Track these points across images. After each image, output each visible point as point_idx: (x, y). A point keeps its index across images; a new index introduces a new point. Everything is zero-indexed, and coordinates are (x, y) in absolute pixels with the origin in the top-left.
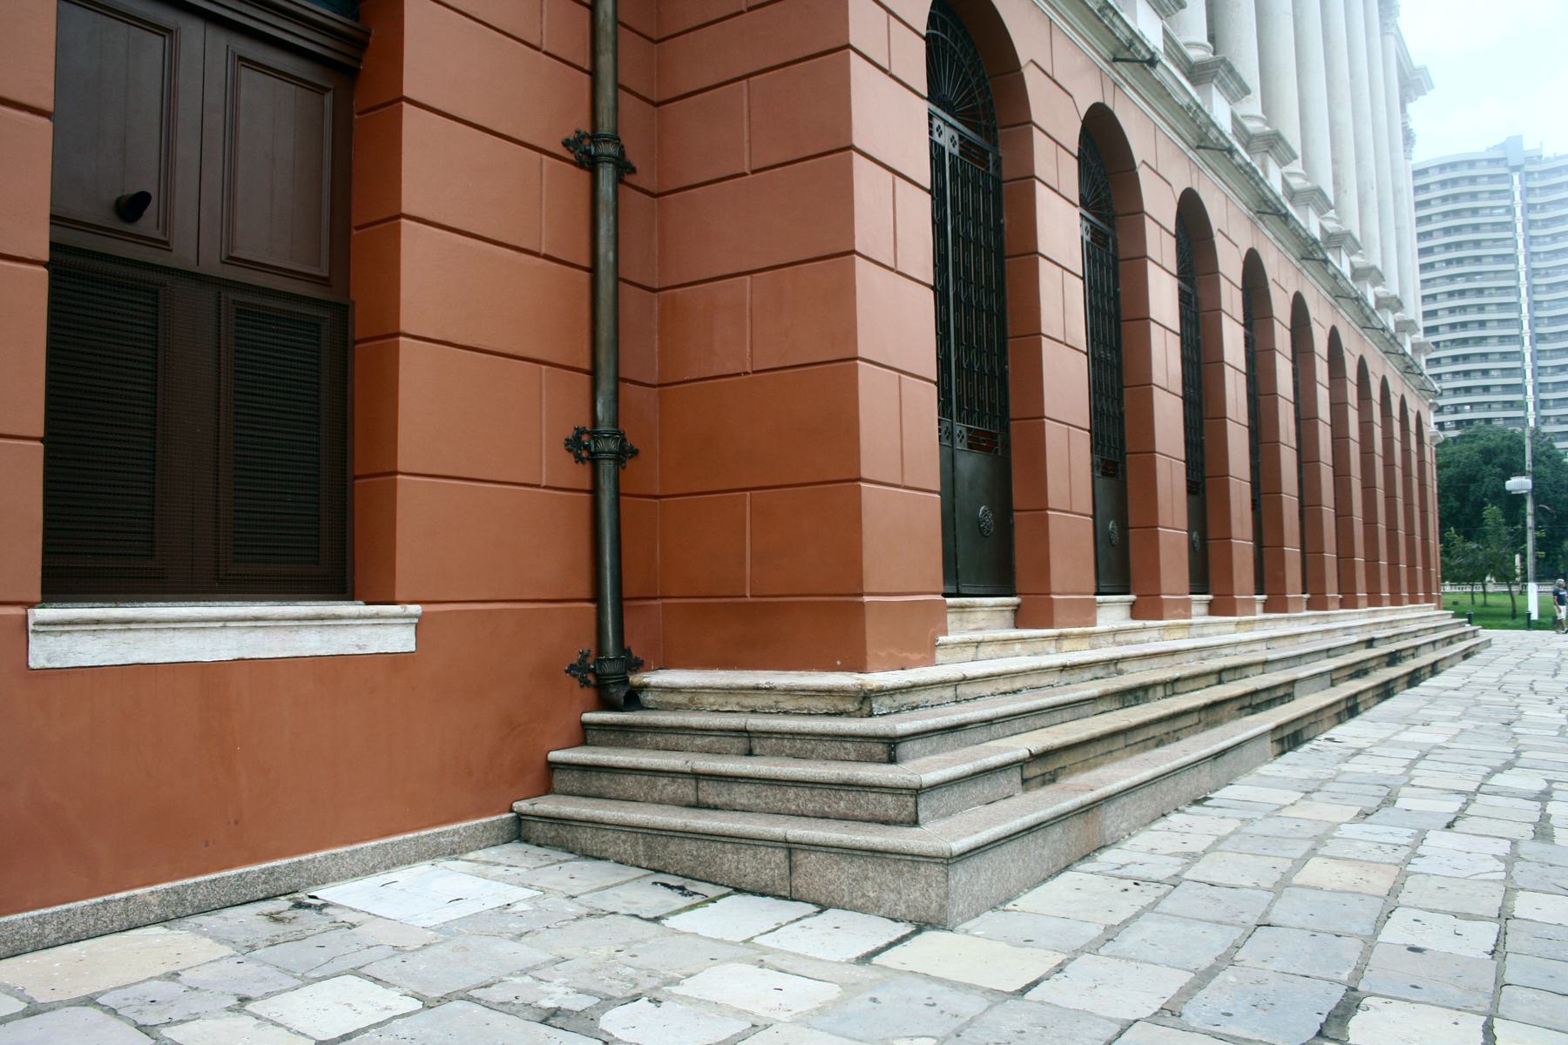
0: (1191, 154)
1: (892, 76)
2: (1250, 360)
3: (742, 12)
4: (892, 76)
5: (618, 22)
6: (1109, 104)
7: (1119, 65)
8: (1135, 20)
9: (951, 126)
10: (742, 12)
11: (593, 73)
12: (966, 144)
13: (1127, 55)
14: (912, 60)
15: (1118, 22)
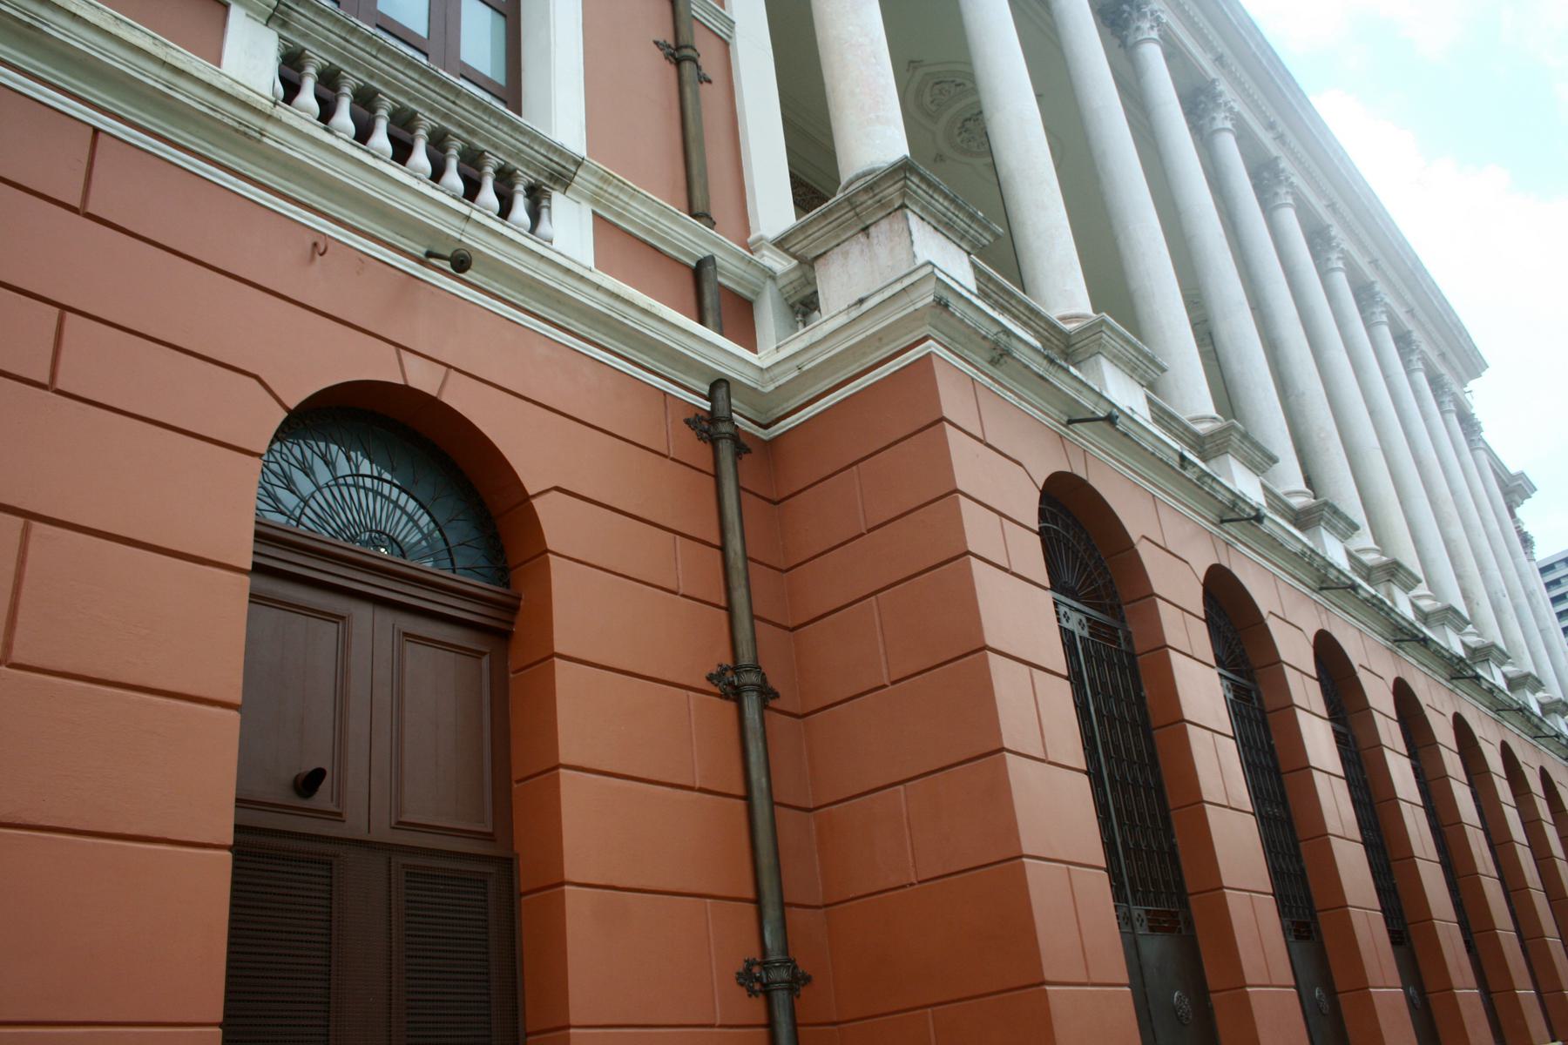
0: (1315, 596)
1: (1013, 574)
2: (1458, 906)
4: (1013, 574)
5: (747, 558)
6: (1226, 564)
7: (1227, 526)
8: (1233, 481)
9: (1077, 610)
11: (729, 609)
12: (1094, 625)
14: (1030, 555)
15: (1217, 487)
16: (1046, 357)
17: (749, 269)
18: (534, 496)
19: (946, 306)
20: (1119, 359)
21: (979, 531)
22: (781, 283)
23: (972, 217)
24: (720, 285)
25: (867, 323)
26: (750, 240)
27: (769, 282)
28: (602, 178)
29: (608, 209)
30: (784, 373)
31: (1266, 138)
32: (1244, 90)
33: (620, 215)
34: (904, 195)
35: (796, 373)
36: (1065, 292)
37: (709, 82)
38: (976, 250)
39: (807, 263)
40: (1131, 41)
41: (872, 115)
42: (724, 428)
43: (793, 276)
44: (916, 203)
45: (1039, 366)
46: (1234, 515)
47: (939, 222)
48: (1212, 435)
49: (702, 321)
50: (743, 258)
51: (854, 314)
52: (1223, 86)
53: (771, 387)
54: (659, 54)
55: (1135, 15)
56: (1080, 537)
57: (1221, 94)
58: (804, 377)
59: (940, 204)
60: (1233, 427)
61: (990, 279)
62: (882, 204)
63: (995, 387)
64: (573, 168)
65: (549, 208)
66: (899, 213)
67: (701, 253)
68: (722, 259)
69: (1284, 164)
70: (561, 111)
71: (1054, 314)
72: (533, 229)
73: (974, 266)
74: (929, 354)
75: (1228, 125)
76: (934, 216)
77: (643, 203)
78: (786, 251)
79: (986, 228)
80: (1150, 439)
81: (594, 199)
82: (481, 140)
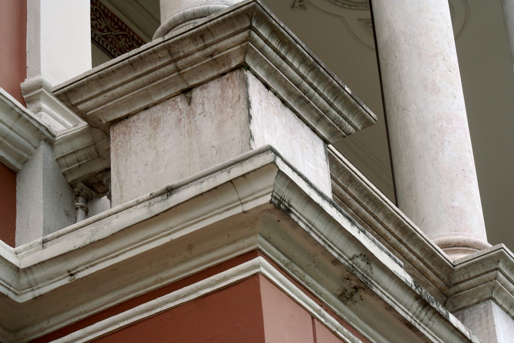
16: (418, 298)
17: (17, 126)
19: (288, 211)
22: (62, 150)
23: (337, 92)
27: (43, 147)
30: (50, 279)
34: (246, 51)
35: (66, 281)
38: (335, 137)
43: (78, 144)
44: (262, 64)
45: (407, 309)
47: (290, 93)
50: (10, 109)
51: (158, 207)
53: (28, 296)
58: (79, 288)
59: (295, 69)
61: (351, 179)
66: (236, 75)
71: (434, 238)
73: (331, 159)
74: (256, 275)
78: (73, 107)
79: (353, 109)
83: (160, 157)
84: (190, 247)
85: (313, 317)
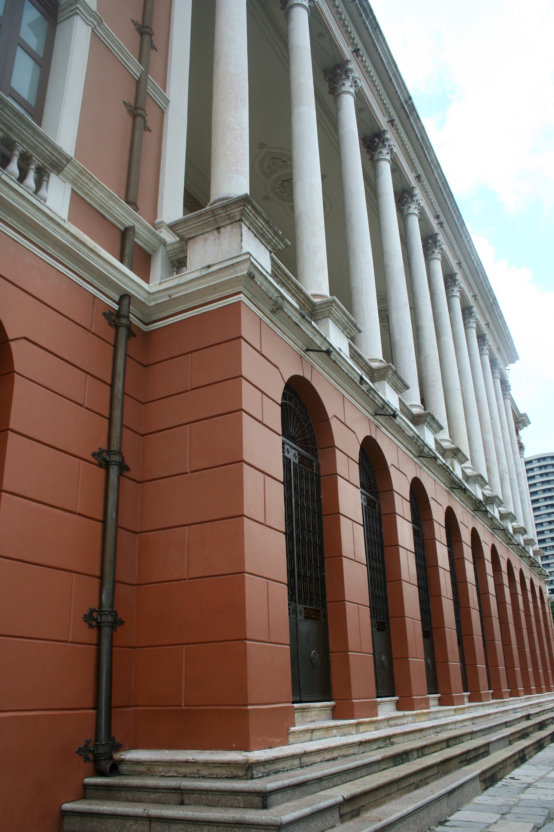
0: (416, 460)
1: (264, 425)
3: (188, 391)
4: (264, 425)
5: (124, 393)
10: (188, 391)
11: (110, 419)
12: (302, 458)
13: (382, 412)
14: (274, 416)
15: (377, 397)
16: (301, 314)
18: (12, 340)
19: (253, 278)
20: (338, 322)
21: (250, 399)
22: (171, 248)
23: (276, 233)
24: (135, 243)
25: (210, 279)
26: (156, 222)
27: (162, 247)
28: (80, 172)
29: (81, 189)
30: (161, 297)
31: (434, 223)
32: (428, 196)
33: (87, 194)
34: (242, 214)
35: (168, 299)
36: (317, 281)
37: (150, 131)
38: (274, 251)
39: (185, 241)
40: (376, 157)
41: (234, 168)
42: (124, 321)
43: (176, 246)
45: (296, 318)
46: (382, 411)
47: (258, 232)
48: (379, 369)
49: (122, 261)
50: (150, 231)
51: (204, 272)
52: (417, 191)
54: (125, 109)
55: (381, 145)
56: (302, 411)
57: (415, 195)
58: (172, 301)
59: (260, 223)
60: (390, 367)
61: (279, 267)
62: (229, 217)
63: (271, 325)
64: (65, 163)
65: (48, 182)
66: (238, 223)
67: (128, 224)
68: (139, 229)
69: (440, 237)
70: (65, 129)
71: (309, 292)
72: (36, 192)
73: (272, 259)
74: (240, 301)
75: (416, 212)
76: (256, 229)
77: (101, 190)
78: (174, 232)
79: (282, 240)
80: (347, 366)
81: (74, 182)
82: (15, 135)
83: (206, 253)
84: (216, 289)
85: (260, 319)
